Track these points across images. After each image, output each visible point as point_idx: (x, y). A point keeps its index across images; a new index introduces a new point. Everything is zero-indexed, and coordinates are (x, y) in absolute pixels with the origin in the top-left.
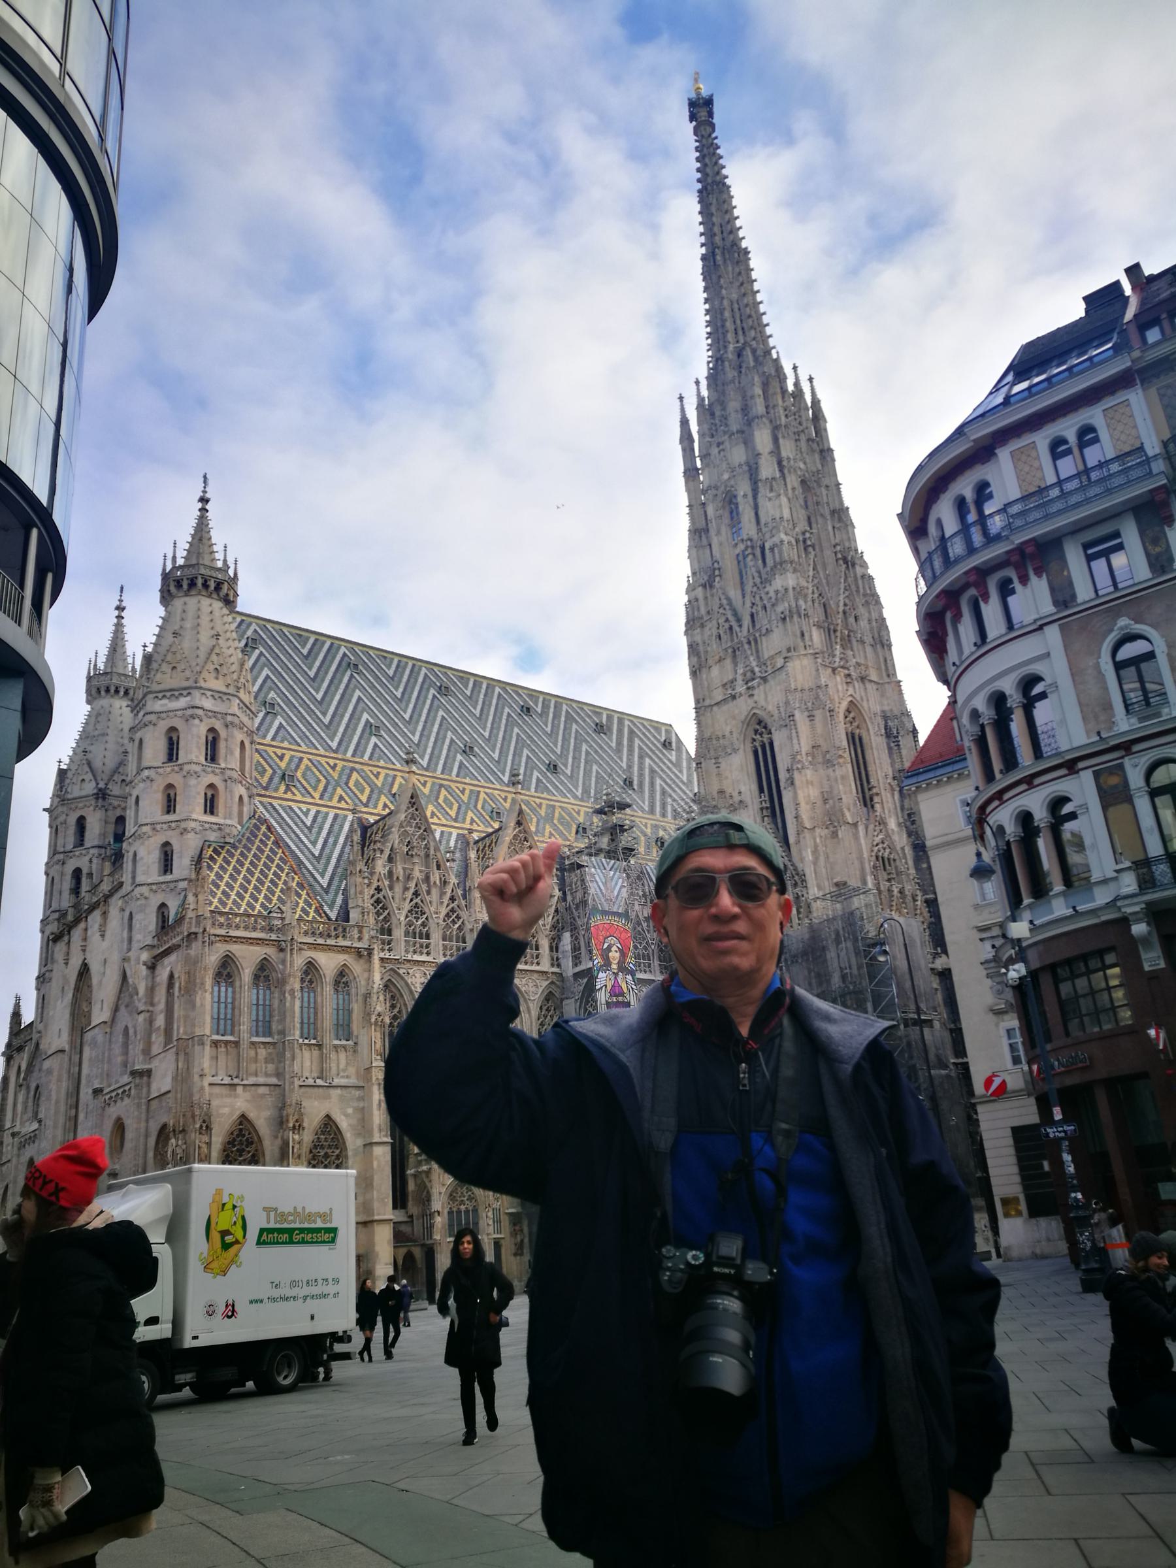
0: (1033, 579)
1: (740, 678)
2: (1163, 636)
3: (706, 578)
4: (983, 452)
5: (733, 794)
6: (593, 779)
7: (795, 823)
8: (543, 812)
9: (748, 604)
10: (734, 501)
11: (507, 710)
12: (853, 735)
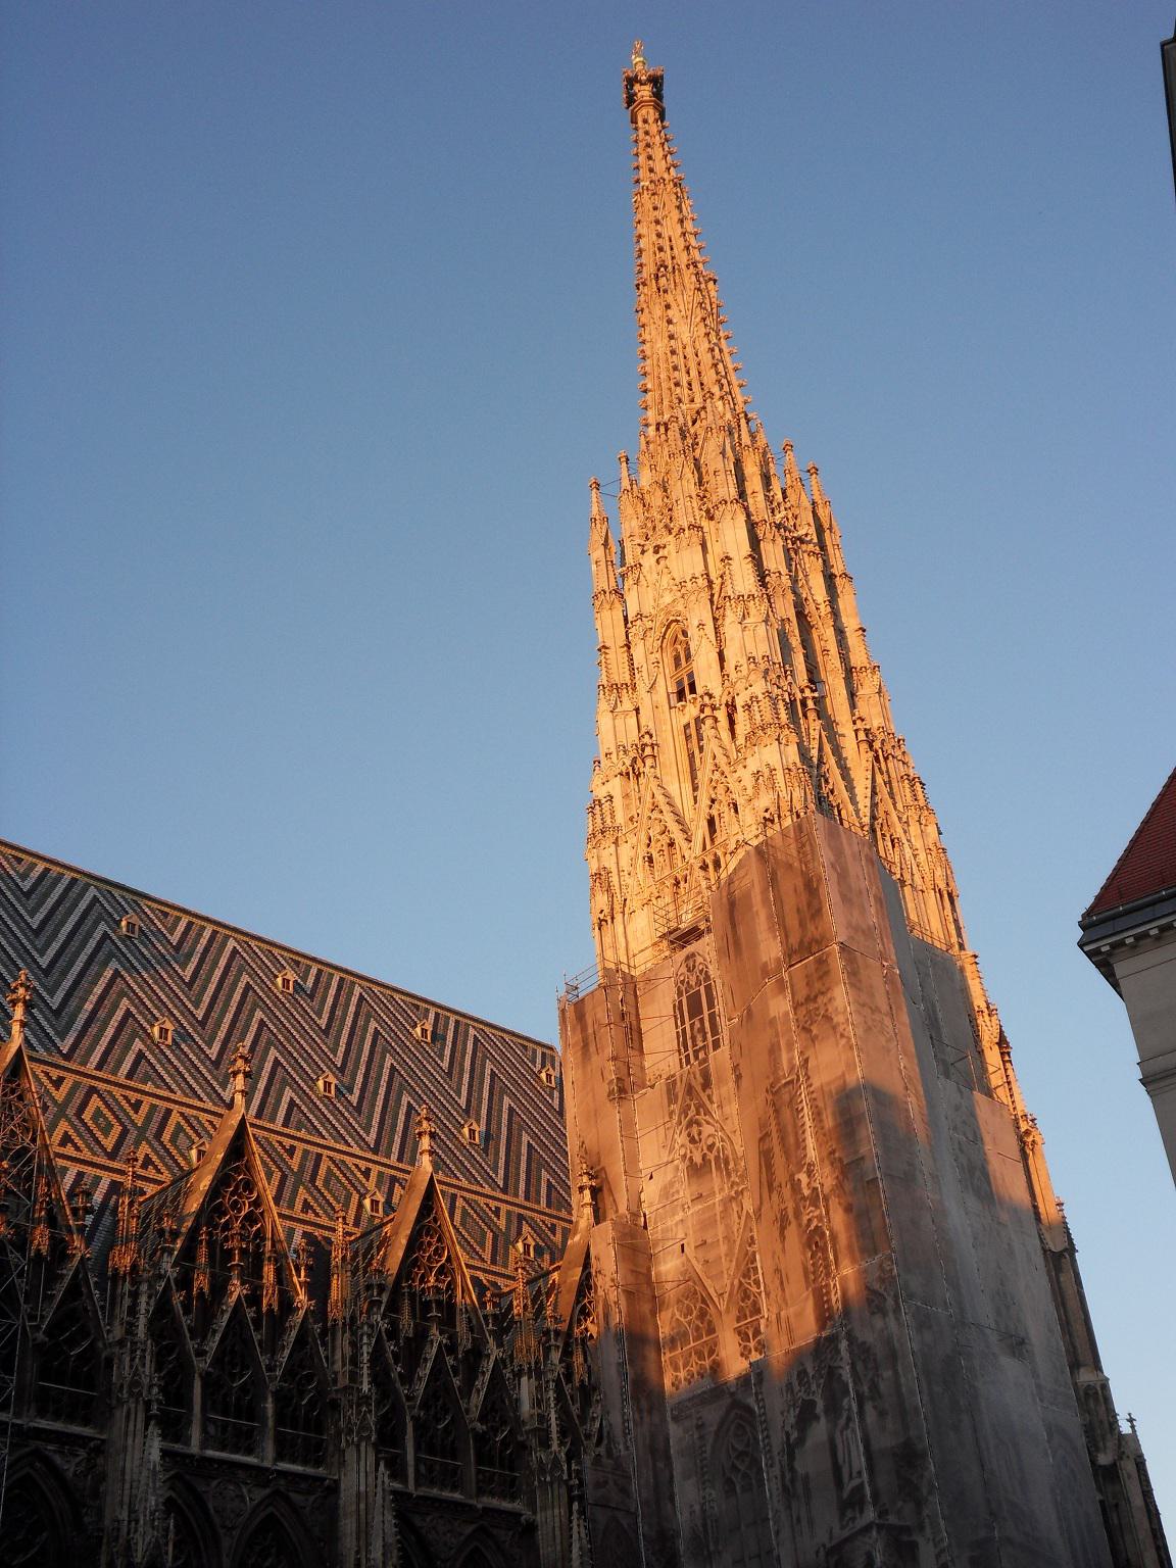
3: (628, 763)
6: (402, 1117)
8: (295, 1163)
9: (704, 802)
11: (245, 978)
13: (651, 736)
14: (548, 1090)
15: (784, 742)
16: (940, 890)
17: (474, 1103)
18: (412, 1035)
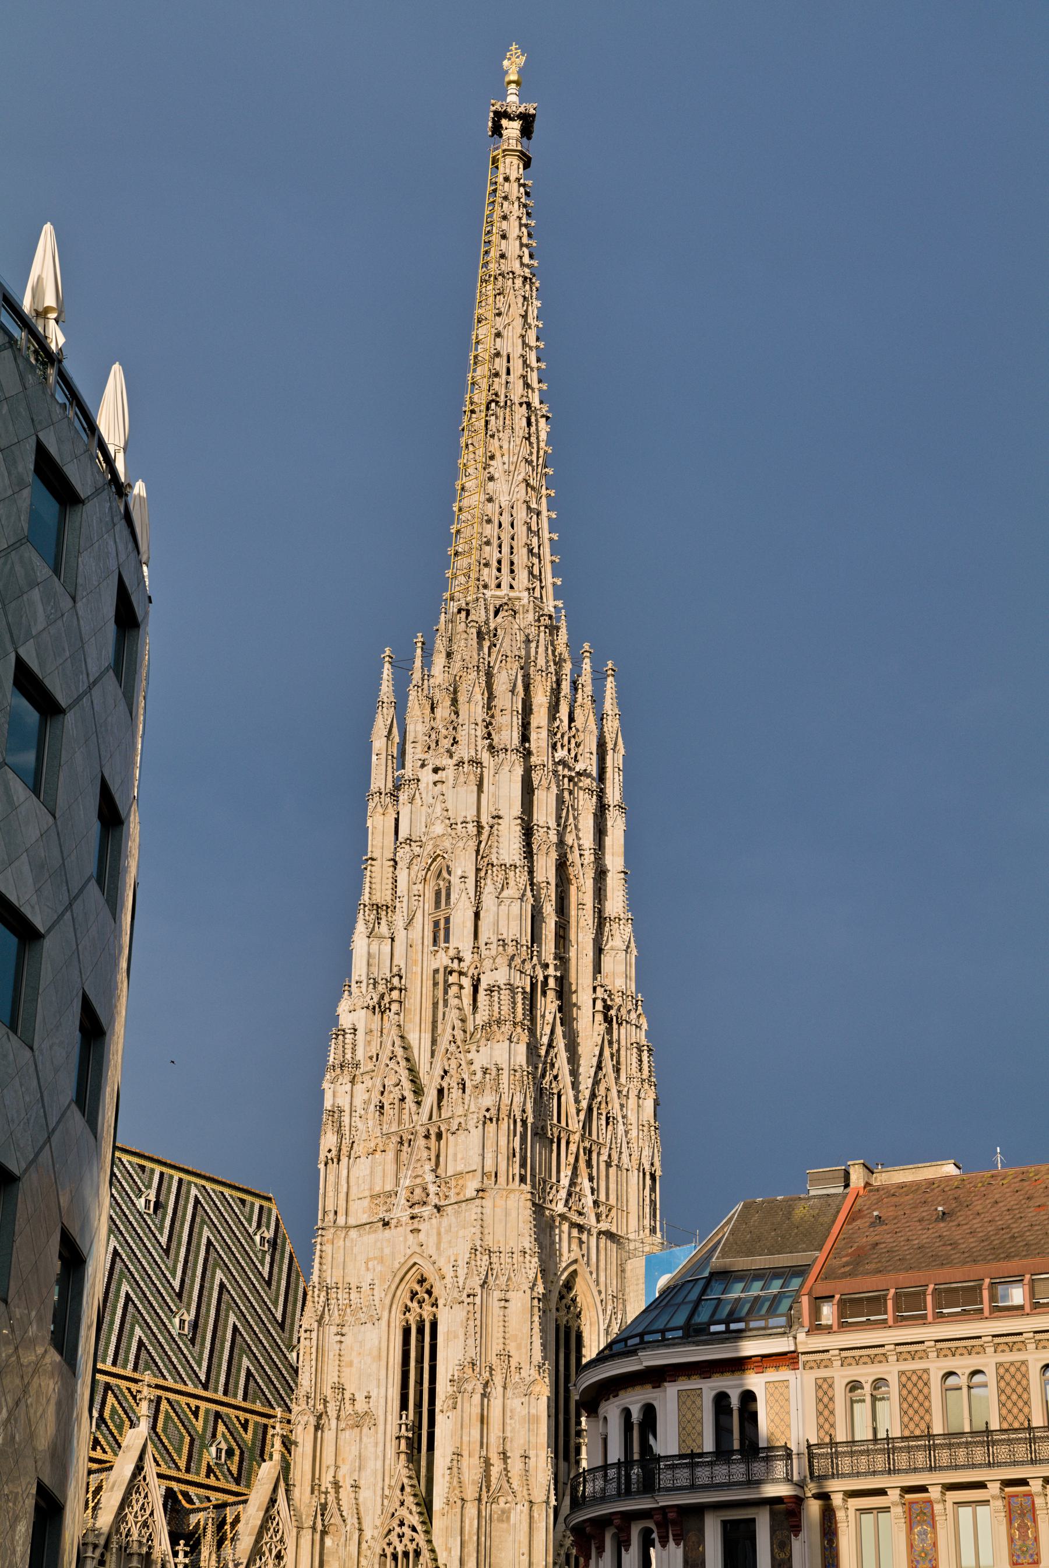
0: (672, 1543)
1: (403, 1194)
3: (376, 1000)
4: (657, 1376)
5: (356, 1397)
7: (447, 1478)
10: (445, 874)
12: (568, 1329)
13: (401, 978)
14: (260, 1255)
15: (515, 1040)
16: (644, 1169)
17: (187, 1286)
18: (134, 1204)
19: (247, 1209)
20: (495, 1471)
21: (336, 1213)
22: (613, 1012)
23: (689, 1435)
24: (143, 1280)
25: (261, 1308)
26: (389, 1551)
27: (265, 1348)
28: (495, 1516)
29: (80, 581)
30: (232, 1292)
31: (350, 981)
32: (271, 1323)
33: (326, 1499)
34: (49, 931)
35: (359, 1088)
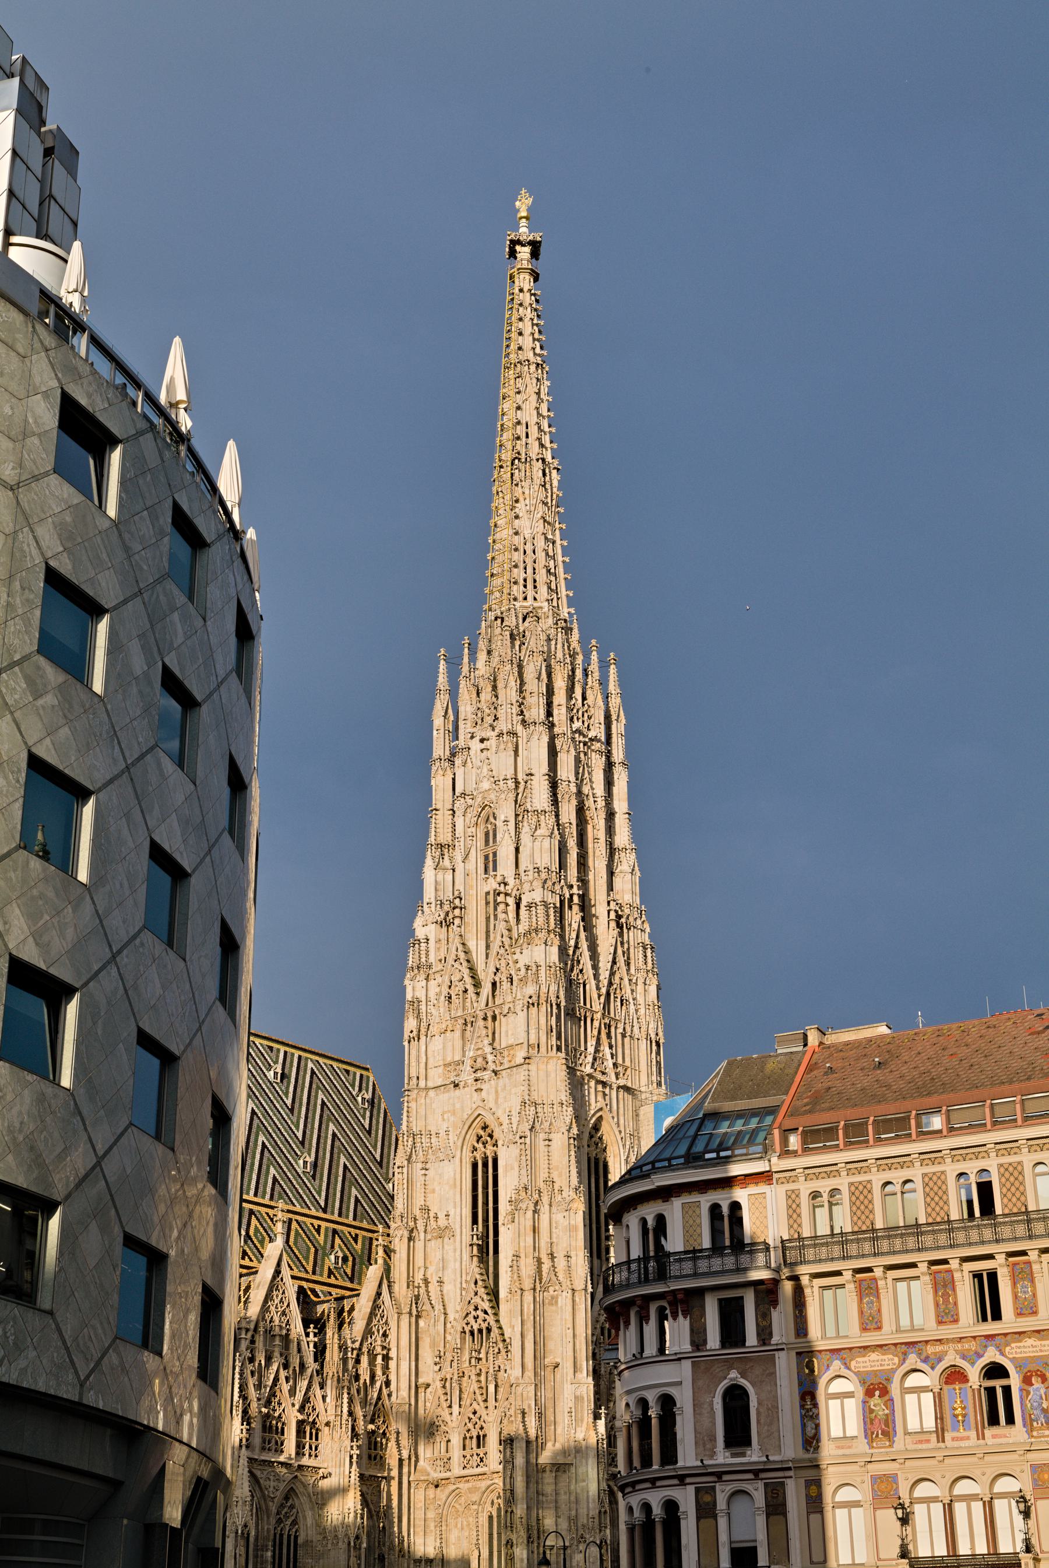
1: (468, 1063)
2: (756, 1394)
3: (442, 916)
4: (666, 1193)
5: (439, 1215)
6: (258, 1156)
7: (509, 1274)
10: (492, 819)
12: (597, 1160)
13: (461, 899)
14: (362, 1111)
15: (549, 943)
17: (308, 1136)
18: (265, 1076)
19: (351, 1077)
20: (546, 1267)
21: (418, 1078)
22: (623, 920)
23: (691, 1236)
24: (275, 1132)
25: (364, 1151)
26: (467, 1329)
27: (368, 1180)
28: (547, 1301)
29: (209, 605)
30: (342, 1140)
31: (422, 903)
32: (372, 1162)
33: (418, 1291)
34: (194, 871)
35: (432, 984)
